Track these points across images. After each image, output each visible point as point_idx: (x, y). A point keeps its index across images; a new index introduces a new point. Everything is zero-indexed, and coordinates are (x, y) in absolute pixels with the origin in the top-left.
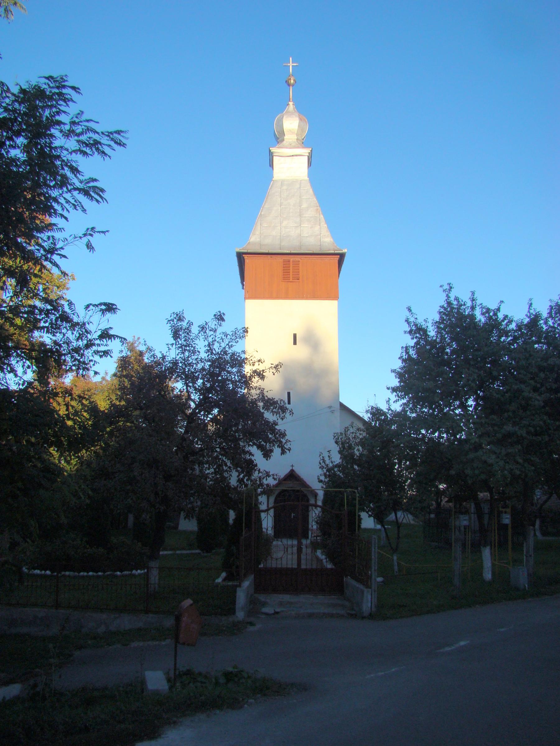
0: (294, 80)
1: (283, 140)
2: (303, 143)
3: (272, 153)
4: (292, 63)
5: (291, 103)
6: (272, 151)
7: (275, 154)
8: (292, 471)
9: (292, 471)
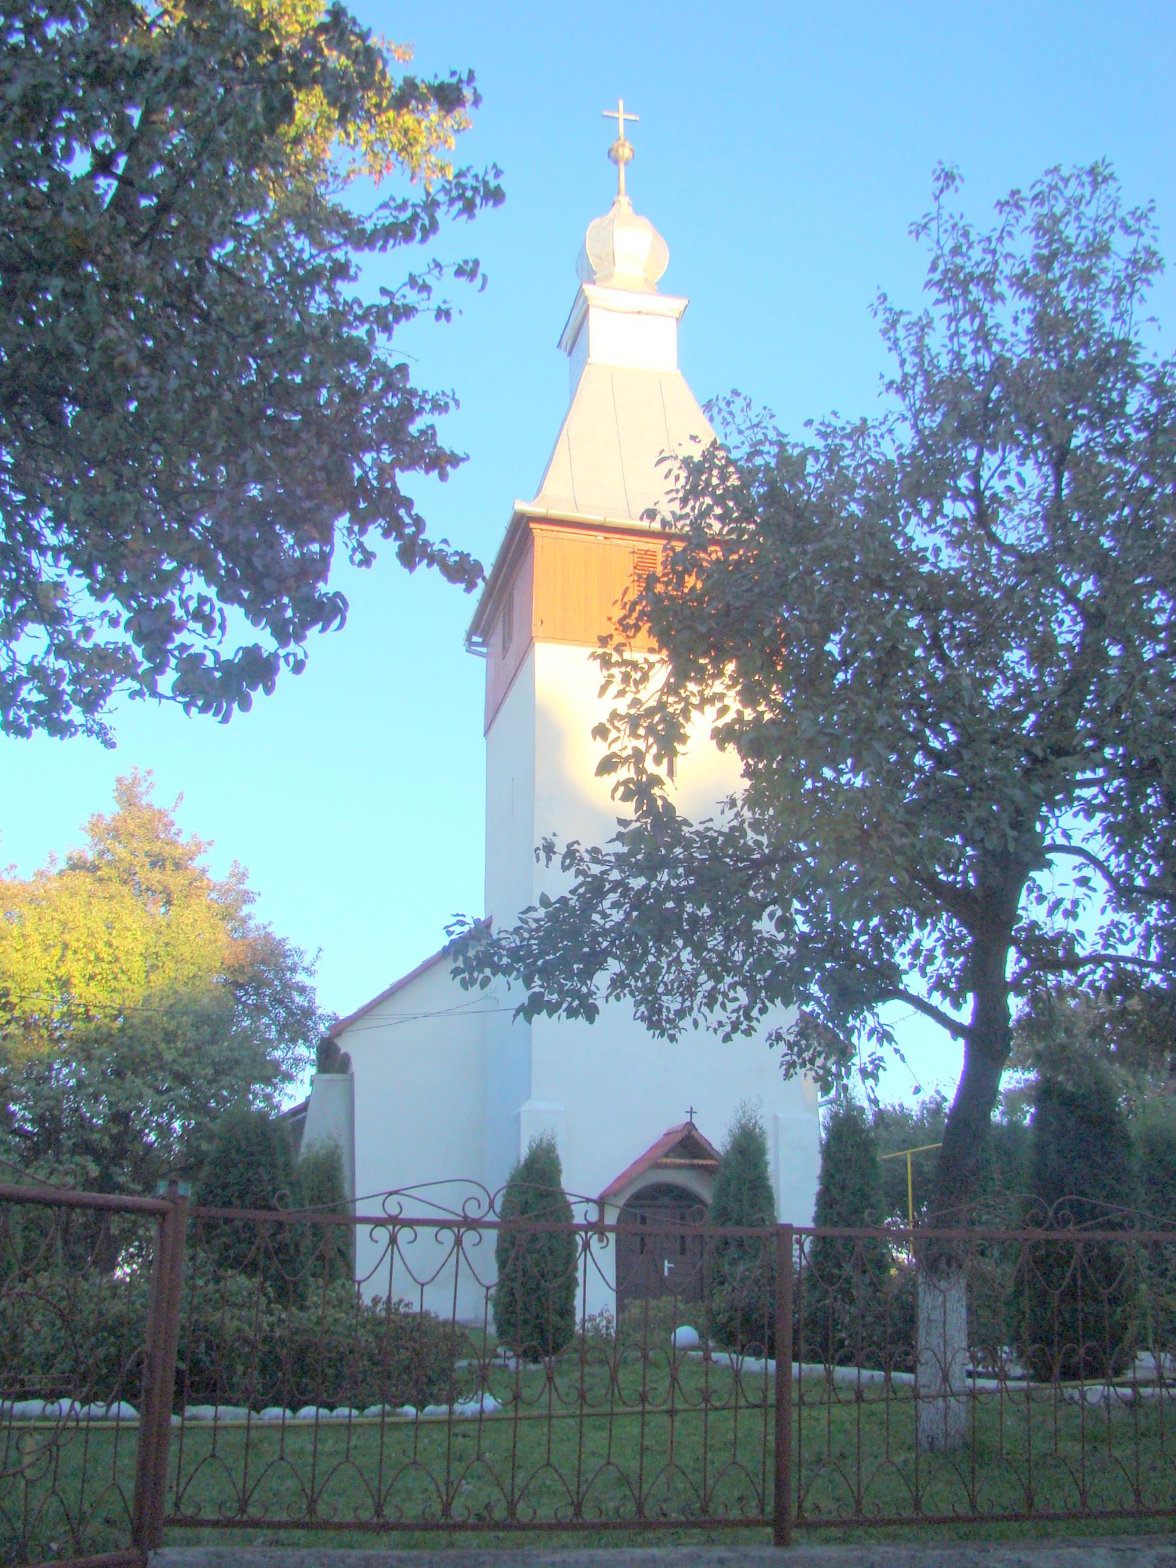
0: (632, 150)
1: (610, 276)
2: (665, 287)
3: (586, 299)
4: (625, 112)
5: (624, 200)
6: (587, 293)
7: (592, 302)
8: (690, 1125)
9: (690, 1125)
